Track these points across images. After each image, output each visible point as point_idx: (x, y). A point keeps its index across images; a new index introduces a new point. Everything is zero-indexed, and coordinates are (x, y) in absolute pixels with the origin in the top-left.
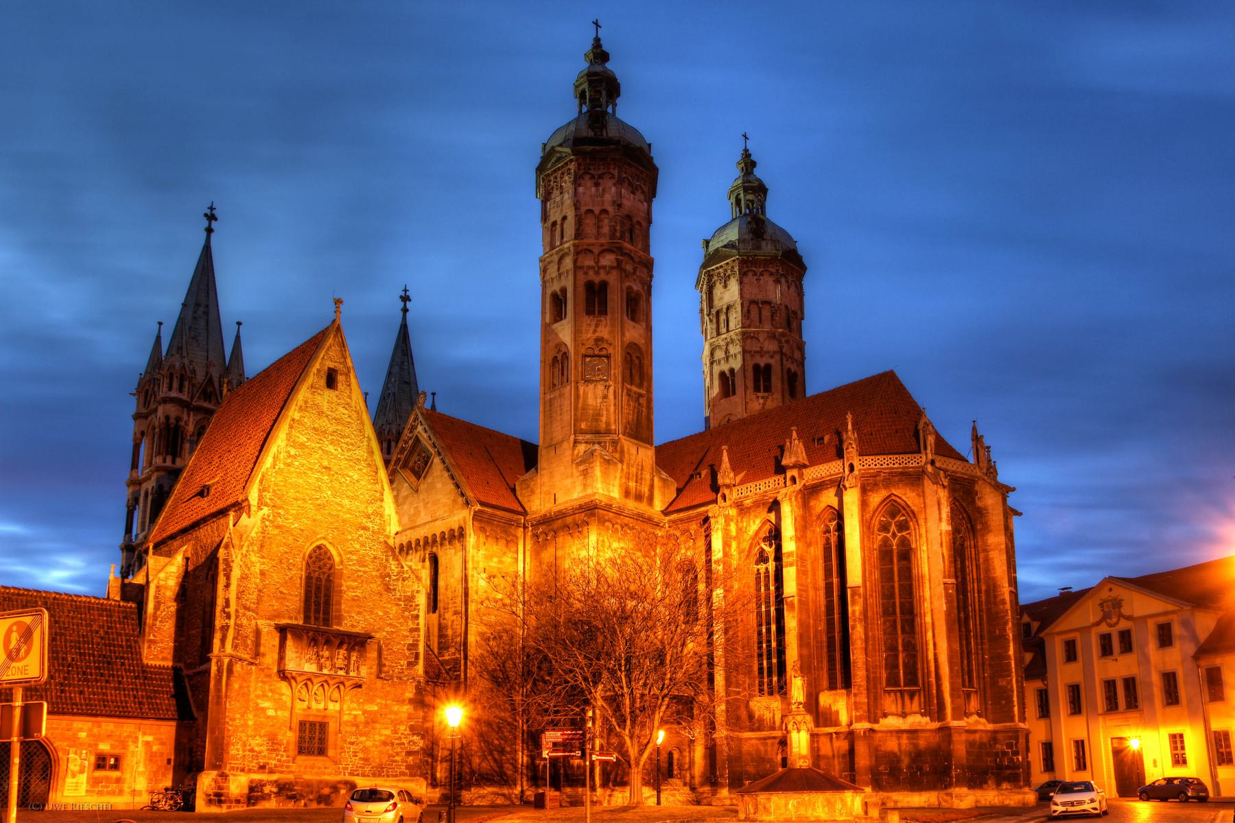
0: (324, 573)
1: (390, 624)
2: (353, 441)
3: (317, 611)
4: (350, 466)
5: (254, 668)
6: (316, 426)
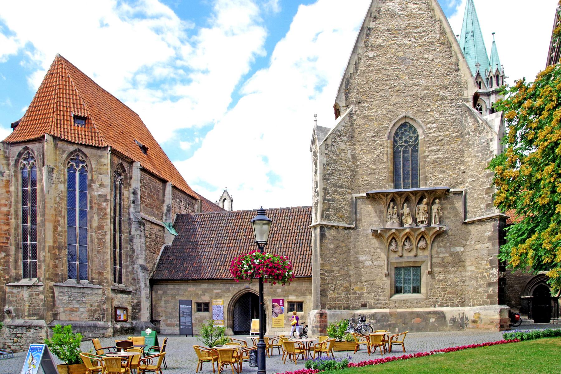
1: (472, 176)
2: (424, 29)
4: (425, 50)
6: (390, 27)
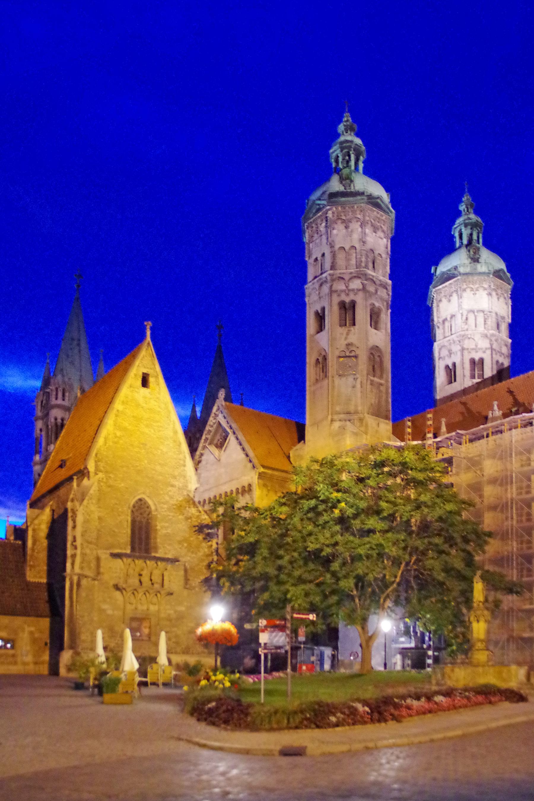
0: (144, 518)
3: (140, 544)
4: (161, 442)
5: (96, 582)
